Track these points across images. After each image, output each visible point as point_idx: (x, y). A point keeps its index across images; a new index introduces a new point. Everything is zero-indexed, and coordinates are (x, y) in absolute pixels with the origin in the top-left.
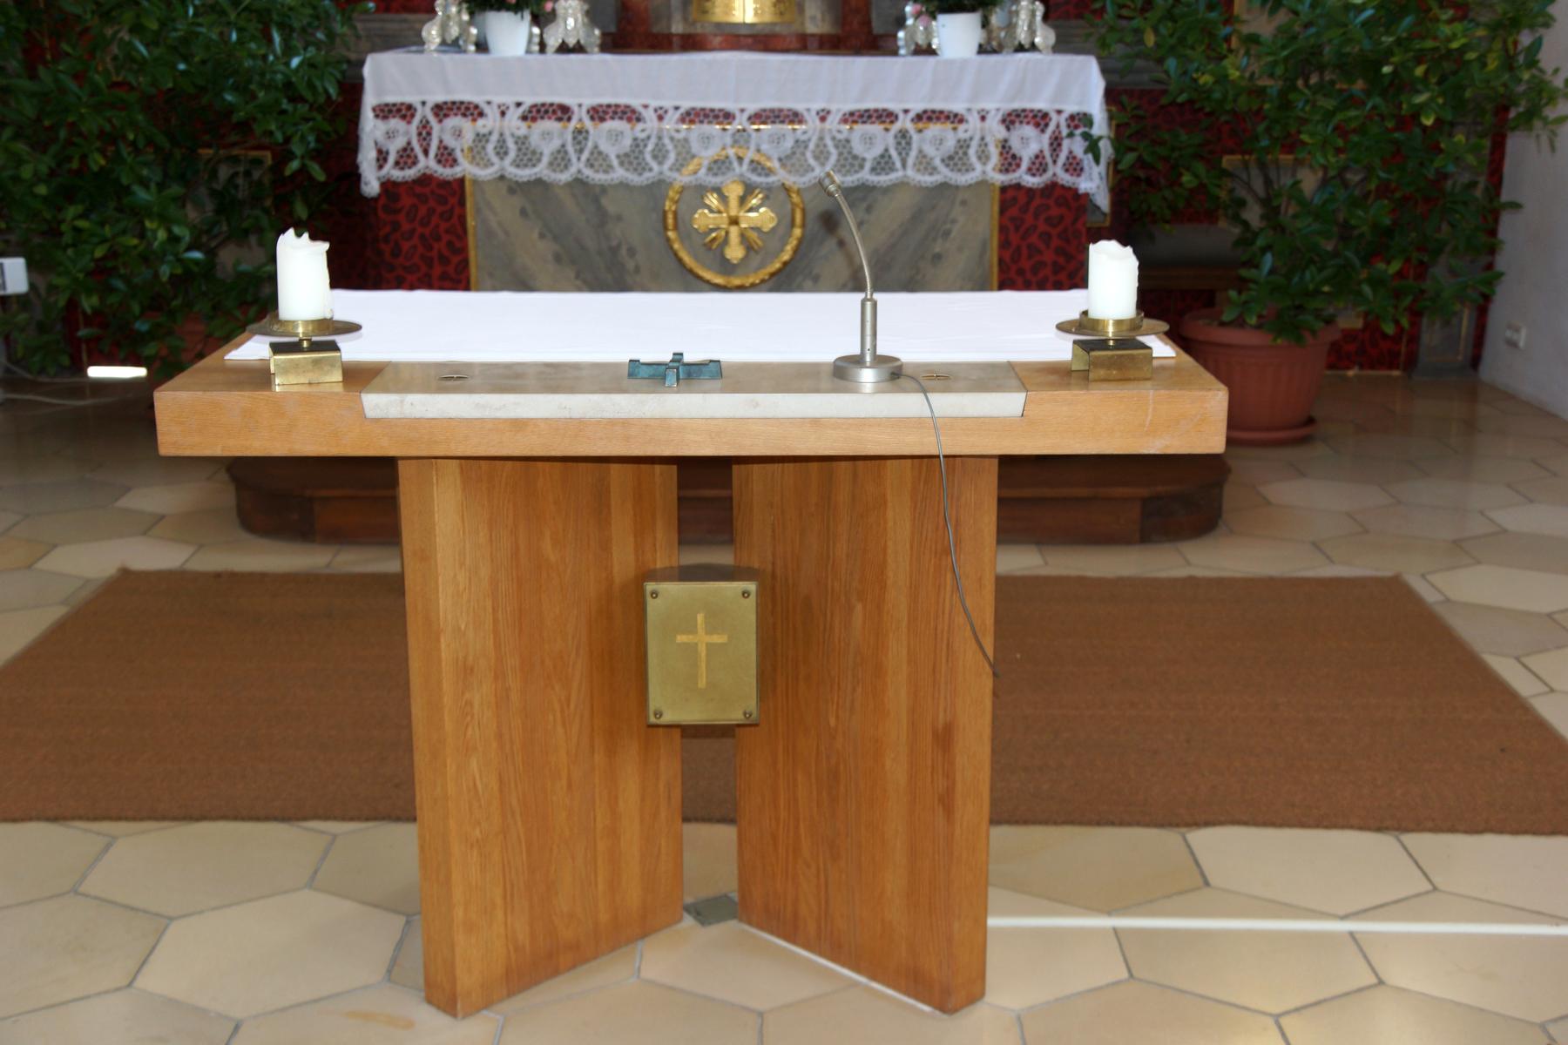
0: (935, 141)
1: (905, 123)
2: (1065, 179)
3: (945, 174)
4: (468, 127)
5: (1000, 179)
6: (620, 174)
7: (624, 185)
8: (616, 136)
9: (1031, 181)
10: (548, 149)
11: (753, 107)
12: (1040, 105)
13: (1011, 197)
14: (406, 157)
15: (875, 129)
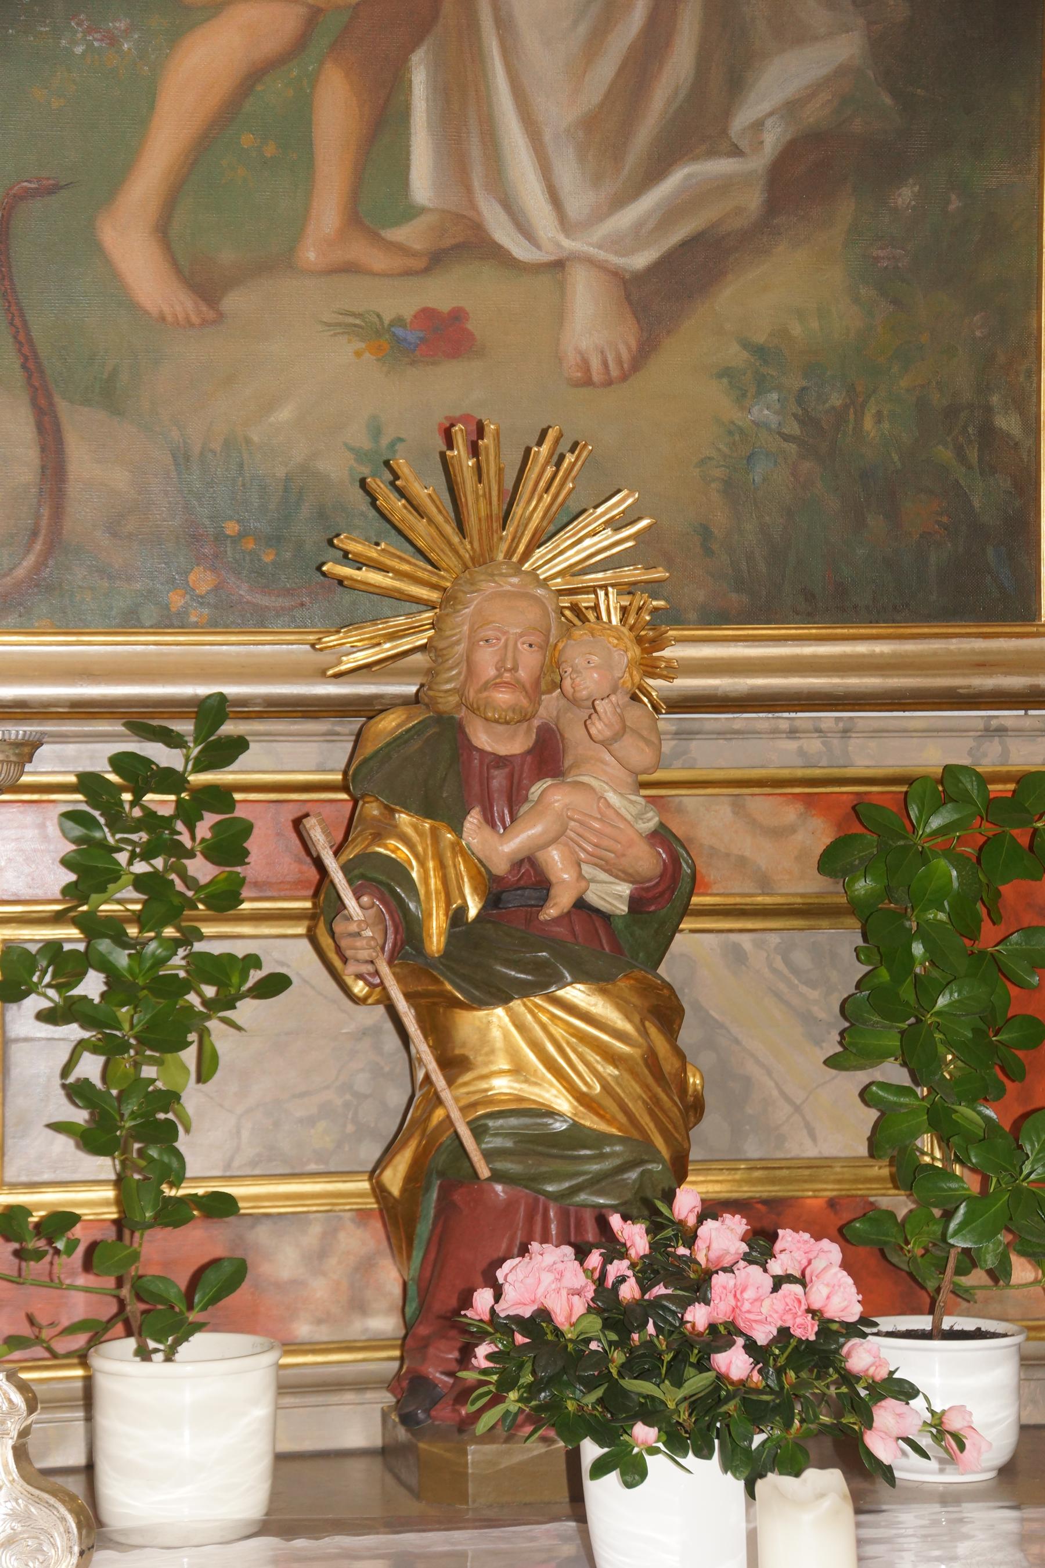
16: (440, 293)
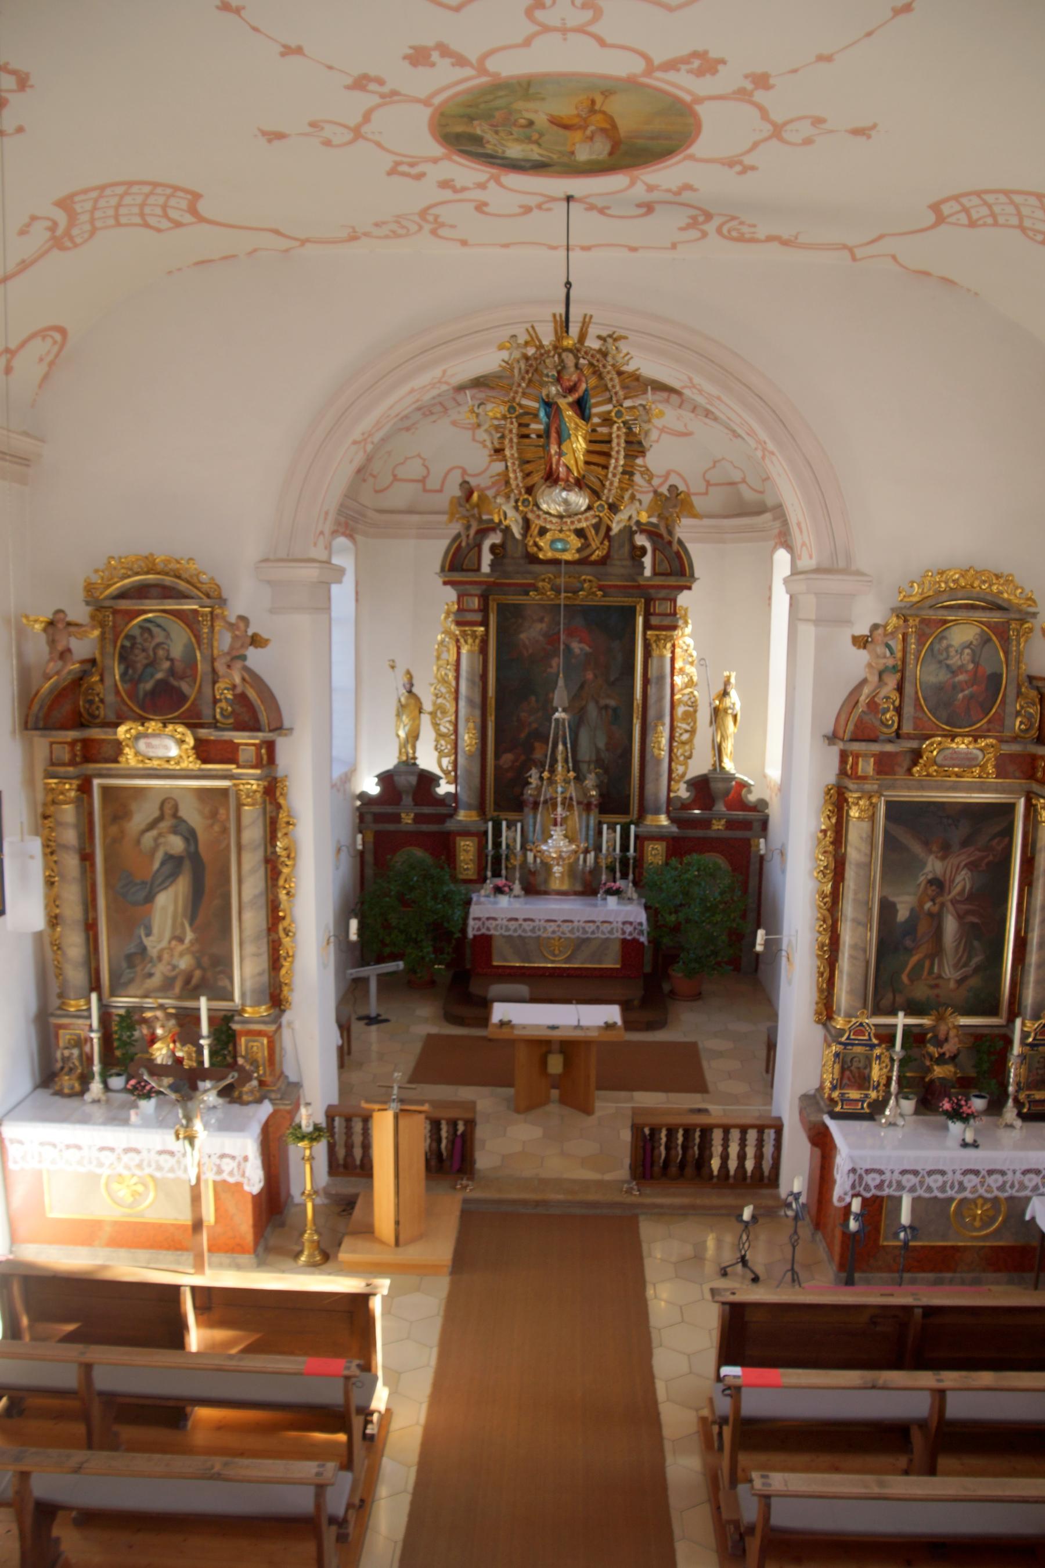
0: (606, 928)
1: (598, 924)
2: (637, 937)
3: (608, 935)
4: (494, 923)
5: (622, 937)
6: (529, 934)
7: (530, 937)
9: (629, 938)
10: (513, 928)
12: (631, 920)
13: (624, 941)
14: (479, 929)
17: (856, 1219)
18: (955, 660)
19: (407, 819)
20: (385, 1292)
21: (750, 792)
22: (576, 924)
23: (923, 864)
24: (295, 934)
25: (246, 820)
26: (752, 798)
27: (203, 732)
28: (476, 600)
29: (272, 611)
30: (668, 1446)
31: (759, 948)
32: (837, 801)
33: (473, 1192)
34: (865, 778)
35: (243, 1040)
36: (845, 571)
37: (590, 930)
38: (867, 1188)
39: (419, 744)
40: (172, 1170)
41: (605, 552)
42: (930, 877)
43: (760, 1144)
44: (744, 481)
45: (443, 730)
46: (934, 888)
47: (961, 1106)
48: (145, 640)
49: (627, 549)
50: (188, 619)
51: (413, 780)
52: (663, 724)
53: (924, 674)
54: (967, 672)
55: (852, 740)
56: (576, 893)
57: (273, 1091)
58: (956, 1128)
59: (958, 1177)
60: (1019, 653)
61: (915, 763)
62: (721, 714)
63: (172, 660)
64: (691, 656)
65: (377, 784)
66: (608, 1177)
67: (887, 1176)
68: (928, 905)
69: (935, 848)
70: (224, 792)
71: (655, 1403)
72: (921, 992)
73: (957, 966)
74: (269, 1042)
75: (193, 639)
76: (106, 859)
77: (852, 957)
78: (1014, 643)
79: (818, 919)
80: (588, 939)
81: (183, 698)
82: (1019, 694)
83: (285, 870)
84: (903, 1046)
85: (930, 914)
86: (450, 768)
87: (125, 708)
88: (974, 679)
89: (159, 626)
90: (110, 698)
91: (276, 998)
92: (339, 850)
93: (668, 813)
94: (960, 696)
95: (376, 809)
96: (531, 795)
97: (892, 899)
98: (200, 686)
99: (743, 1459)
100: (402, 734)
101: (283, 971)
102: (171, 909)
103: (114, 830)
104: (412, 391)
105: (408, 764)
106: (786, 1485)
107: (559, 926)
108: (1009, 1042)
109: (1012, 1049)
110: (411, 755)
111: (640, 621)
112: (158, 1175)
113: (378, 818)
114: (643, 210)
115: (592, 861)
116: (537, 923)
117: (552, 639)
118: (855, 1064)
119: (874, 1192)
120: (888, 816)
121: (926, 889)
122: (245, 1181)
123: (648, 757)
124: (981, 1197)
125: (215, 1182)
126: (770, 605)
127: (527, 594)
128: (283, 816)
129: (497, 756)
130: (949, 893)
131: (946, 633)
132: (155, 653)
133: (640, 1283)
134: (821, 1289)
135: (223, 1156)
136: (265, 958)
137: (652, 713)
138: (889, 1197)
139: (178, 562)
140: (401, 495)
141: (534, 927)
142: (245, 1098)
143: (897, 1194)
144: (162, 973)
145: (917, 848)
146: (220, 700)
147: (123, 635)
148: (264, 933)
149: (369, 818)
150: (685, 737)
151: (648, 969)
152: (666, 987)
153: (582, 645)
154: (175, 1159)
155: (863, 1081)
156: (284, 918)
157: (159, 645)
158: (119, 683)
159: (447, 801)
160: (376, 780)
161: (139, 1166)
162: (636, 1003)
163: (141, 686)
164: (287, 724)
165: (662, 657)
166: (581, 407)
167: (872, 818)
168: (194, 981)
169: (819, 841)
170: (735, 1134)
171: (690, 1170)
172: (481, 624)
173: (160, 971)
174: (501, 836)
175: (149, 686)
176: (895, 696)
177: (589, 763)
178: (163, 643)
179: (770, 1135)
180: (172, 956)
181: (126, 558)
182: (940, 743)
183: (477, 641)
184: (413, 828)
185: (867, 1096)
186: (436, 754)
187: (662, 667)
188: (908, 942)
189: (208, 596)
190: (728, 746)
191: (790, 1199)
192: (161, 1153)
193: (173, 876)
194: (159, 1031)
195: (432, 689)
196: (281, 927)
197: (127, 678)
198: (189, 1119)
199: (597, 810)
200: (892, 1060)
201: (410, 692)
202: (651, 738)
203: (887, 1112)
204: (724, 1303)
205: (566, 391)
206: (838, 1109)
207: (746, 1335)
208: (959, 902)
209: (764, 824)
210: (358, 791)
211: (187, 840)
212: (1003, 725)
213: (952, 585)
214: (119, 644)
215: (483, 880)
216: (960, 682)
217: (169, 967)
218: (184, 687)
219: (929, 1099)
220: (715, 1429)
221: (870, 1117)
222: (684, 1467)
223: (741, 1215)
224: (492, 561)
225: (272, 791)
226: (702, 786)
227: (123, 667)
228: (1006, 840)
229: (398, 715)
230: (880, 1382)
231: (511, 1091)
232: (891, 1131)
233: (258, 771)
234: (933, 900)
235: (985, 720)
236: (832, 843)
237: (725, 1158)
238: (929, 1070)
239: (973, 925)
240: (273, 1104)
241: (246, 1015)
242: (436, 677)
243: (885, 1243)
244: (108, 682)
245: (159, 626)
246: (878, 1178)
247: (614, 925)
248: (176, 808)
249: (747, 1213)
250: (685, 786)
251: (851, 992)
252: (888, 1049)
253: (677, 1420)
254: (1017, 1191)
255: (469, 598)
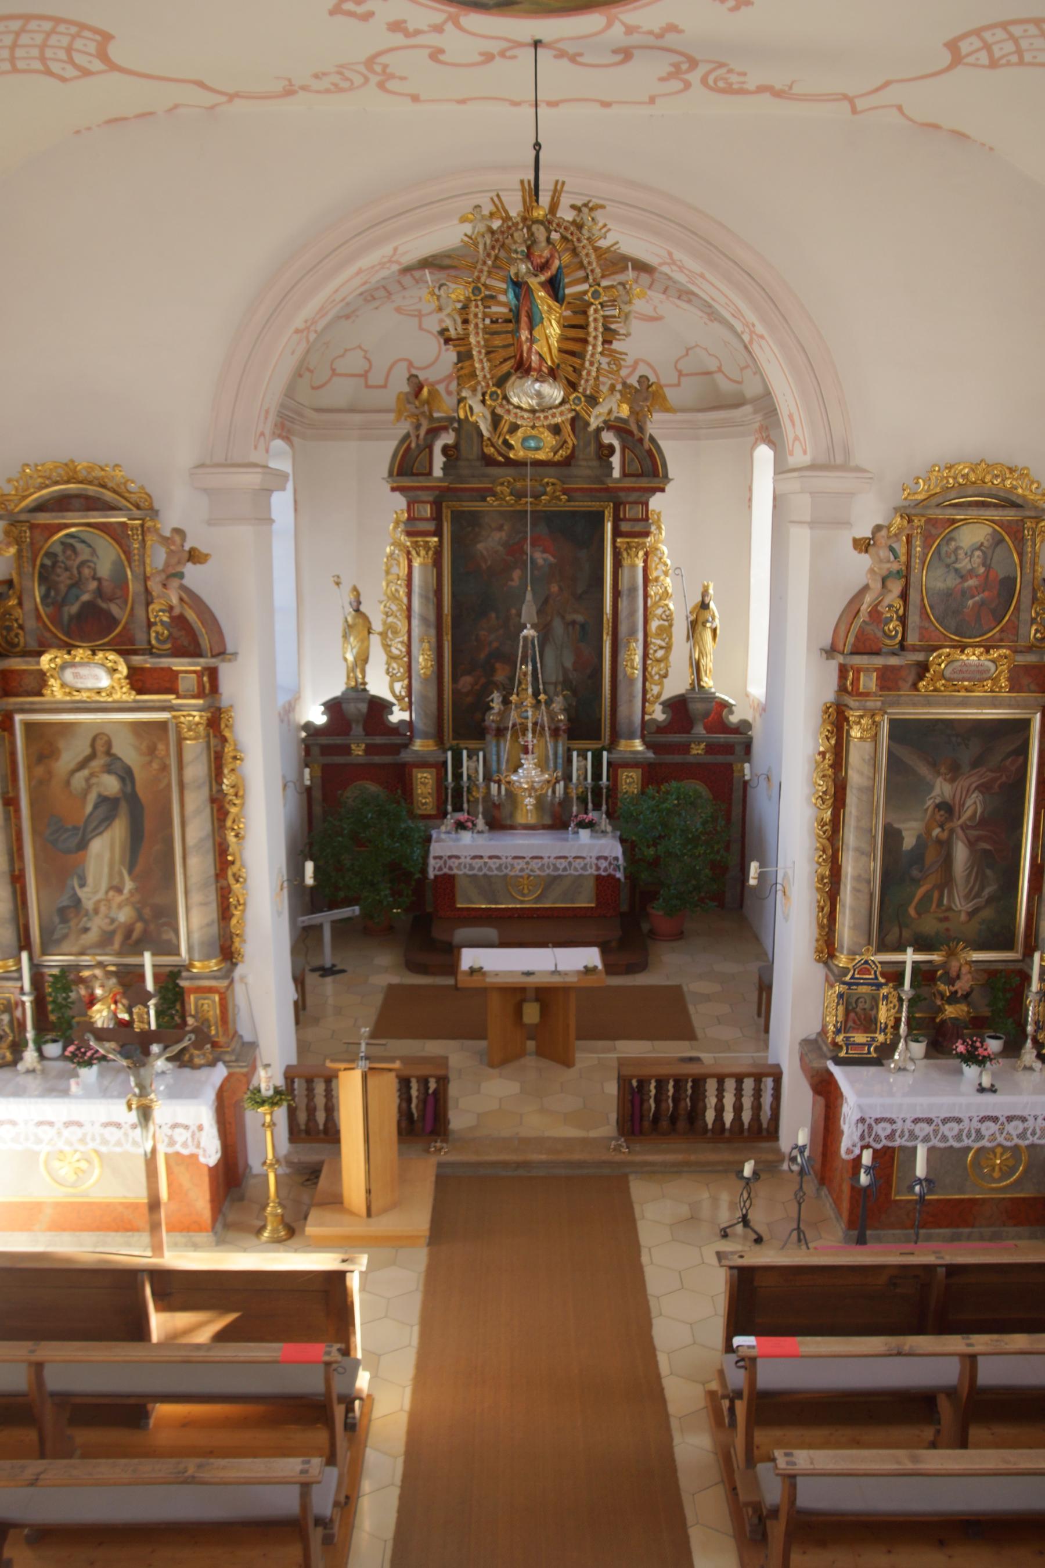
1: (570, 859)
2: (613, 873)
3: (581, 872)
4: (457, 861)
5: (596, 873)
6: (496, 872)
7: (496, 876)
8: (495, 863)
9: (604, 874)
10: (477, 867)
11: (531, 855)
12: (606, 854)
13: (598, 878)
14: (440, 869)
15: (563, 861)
16: (947, 914)
17: (867, 1173)
18: (964, 563)
19: (358, 750)
20: (364, 1269)
21: (731, 712)
22: (546, 860)
23: (931, 788)
24: (245, 880)
25: (188, 756)
26: (734, 719)
27: (137, 660)
28: (428, 507)
29: (211, 522)
30: (674, 1424)
31: (752, 882)
32: (837, 720)
33: (449, 1155)
34: (867, 694)
35: (192, 997)
36: (844, 467)
37: (561, 867)
38: (877, 1139)
39: (369, 668)
40: (119, 1143)
41: (569, 452)
42: (937, 801)
43: (758, 1093)
44: (720, 370)
45: (395, 652)
46: (942, 812)
47: (976, 1048)
48: (68, 558)
49: (592, 448)
50: (117, 534)
51: (364, 707)
52: (636, 641)
53: (931, 580)
54: (977, 576)
55: (852, 653)
56: (545, 827)
57: (227, 1052)
58: (971, 1072)
59: (975, 1124)
60: (1035, 554)
61: (921, 677)
62: (700, 627)
63: (99, 580)
64: (666, 565)
65: (323, 713)
66: (593, 1134)
67: (899, 1126)
68: (936, 832)
69: (943, 770)
70: (163, 725)
71: (658, 1377)
72: (929, 925)
73: (968, 897)
74: (221, 999)
75: (123, 556)
76: (32, 804)
77: (855, 890)
78: (1029, 543)
79: (817, 849)
80: (560, 877)
81: (114, 622)
82: (1034, 599)
83: (233, 810)
84: (912, 986)
85: (939, 842)
86: (403, 694)
87: (48, 635)
88: (985, 585)
89: (83, 542)
90: (31, 624)
91: (227, 951)
92: (285, 786)
93: (643, 737)
94: (970, 602)
95: (324, 740)
96: (493, 721)
97: (896, 826)
98: (132, 609)
99: (761, 1436)
100: (350, 657)
101: (234, 921)
102: (107, 856)
103: (39, 771)
104: (359, 272)
105: (358, 690)
106: (812, 1463)
107: (527, 863)
108: (1027, 978)
109: (1030, 985)
110: (360, 680)
111: (609, 527)
112: (104, 1149)
113: (326, 750)
114: (619, 57)
115: (562, 792)
116: (504, 860)
117: (515, 550)
118: (861, 1005)
119: (884, 1142)
120: (891, 736)
121: (934, 813)
122: (200, 1152)
123: (620, 677)
124: (999, 1145)
125: (166, 1154)
126: (750, 507)
127: (484, 499)
128: (228, 749)
129: (455, 679)
130: (959, 818)
131: (954, 534)
132: (79, 573)
133: (634, 1247)
134: (830, 1249)
135: (175, 1126)
136: (214, 906)
137: (623, 629)
138: (902, 1148)
139: (103, 470)
140: (342, 391)
141: (501, 865)
142: (197, 1061)
143: (910, 1144)
144: (100, 927)
145: (923, 770)
146: (155, 624)
147: (42, 552)
148: (213, 880)
149: (316, 751)
150: (660, 654)
151: (624, 908)
152: (645, 927)
153: (545, 555)
154: (123, 1130)
155: (869, 1024)
156: (233, 863)
157: (83, 563)
158: (40, 607)
159: (402, 730)
160: (322, 708)
161: (83, 1140)
162: (614, 944)
163: (66, 609)
164: (230, 648)
165: (633, 566)
166: (554, 287)
167: (875, 738)
168: (135, 935)
169: (817, 764)
170: (730, 1084)
171: (682, 1124)
172: (434, 535)
173: (97, 925)
174: (461, 766)
175: (74, 609)
176: (898, 604)
177: (556, 684)
178: (88, 561)
179: (769, 1082)
180: (109, 908)
181: (43, 465)
182: (948, 655)
183: (431, 553)
184: (363, 760)
185: (873, 1039)
186: (388, 678)
187: (633, 578)
188: (915, 873)
189: (138, 507)
190: (708, 663)
191: (795, 1152)
192: (106, 1125)
193: (108, 819)
194: (99, 992)
195: (382, 607)
196: (230, 873)
197: (49, 601)
198: (143, 1090)
199: (565, 736)
200: (900, 1000)
201: (357, 610)
202: (623, 655)
203: (896, 1057)
204: (731, 1268)
205: (537, 270)
206: (842, 1054)
207: (757, 1302)
208: (969, 827)
209: (748, 747)
210: (303, 722)
211: (122, 779)
212: (1017, 635)
213: (961, 480)
214: (38, 563)
215: (445, 815)
216: (970, 588)
217: (107, 921)
218: (115, 609)
219: (939, 1039)
220: (726, 1404)
221: (877, 1062)
222: (693, 1446)
223: (742, 1171)
224: (445, 463)
225: (217, 723)
226: (678, 706)
227: (43, 589)
228: (1021, 759)
229: (345, 636)
230: (906, 1349)
231: (483, 1044)
232: (901, 1077)
233: (201, 701)
234: (942, 826)
235: (998, 629)
236: (831, 766)
237: (720, 1109)
238: (941, 1010)
239: (985, 852)
240: (228, 1067)
241: (195, 970)
242: (386, 594)
243: (898, 1198)
244: (28, 605)
245: (83, 542)
246: (888, 1128)
247: (588, 860)
248: (109, 744)
249: (748, 1170)
250: (661, 707)
251: (854, 927)
252: (895, 988)
253: (683, 1394)
254: (1039, 1138)
255: (421, 506)
